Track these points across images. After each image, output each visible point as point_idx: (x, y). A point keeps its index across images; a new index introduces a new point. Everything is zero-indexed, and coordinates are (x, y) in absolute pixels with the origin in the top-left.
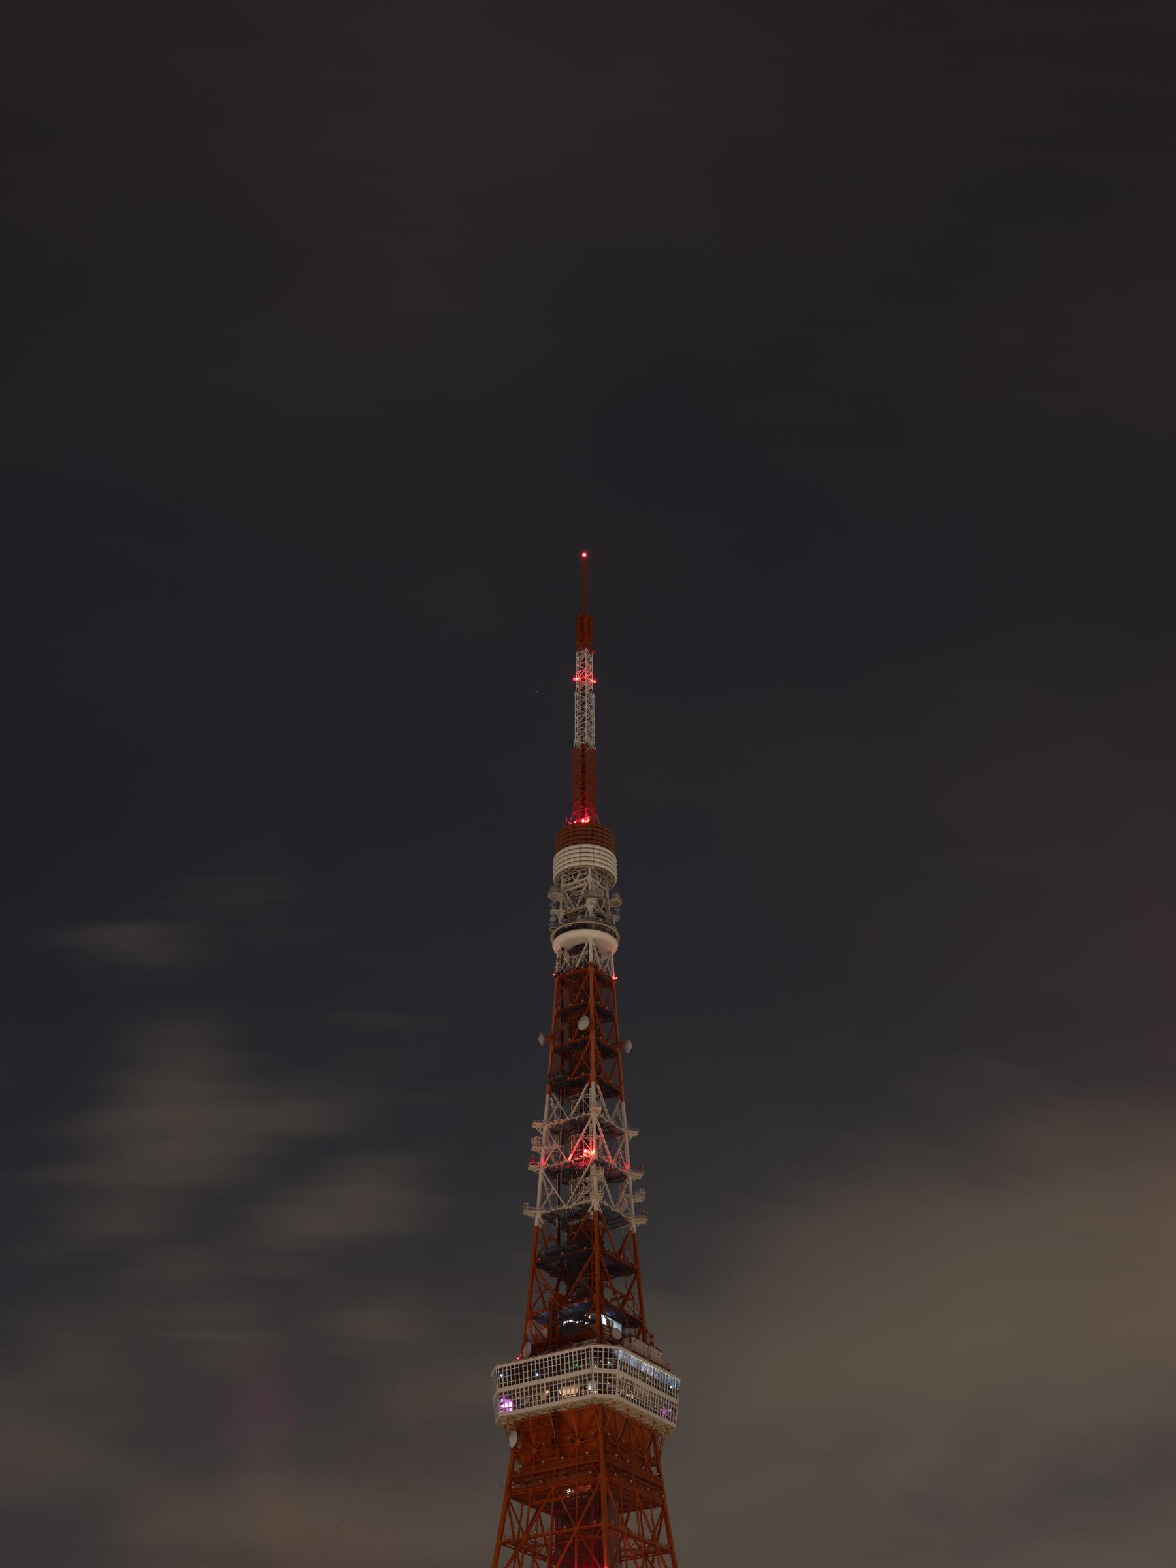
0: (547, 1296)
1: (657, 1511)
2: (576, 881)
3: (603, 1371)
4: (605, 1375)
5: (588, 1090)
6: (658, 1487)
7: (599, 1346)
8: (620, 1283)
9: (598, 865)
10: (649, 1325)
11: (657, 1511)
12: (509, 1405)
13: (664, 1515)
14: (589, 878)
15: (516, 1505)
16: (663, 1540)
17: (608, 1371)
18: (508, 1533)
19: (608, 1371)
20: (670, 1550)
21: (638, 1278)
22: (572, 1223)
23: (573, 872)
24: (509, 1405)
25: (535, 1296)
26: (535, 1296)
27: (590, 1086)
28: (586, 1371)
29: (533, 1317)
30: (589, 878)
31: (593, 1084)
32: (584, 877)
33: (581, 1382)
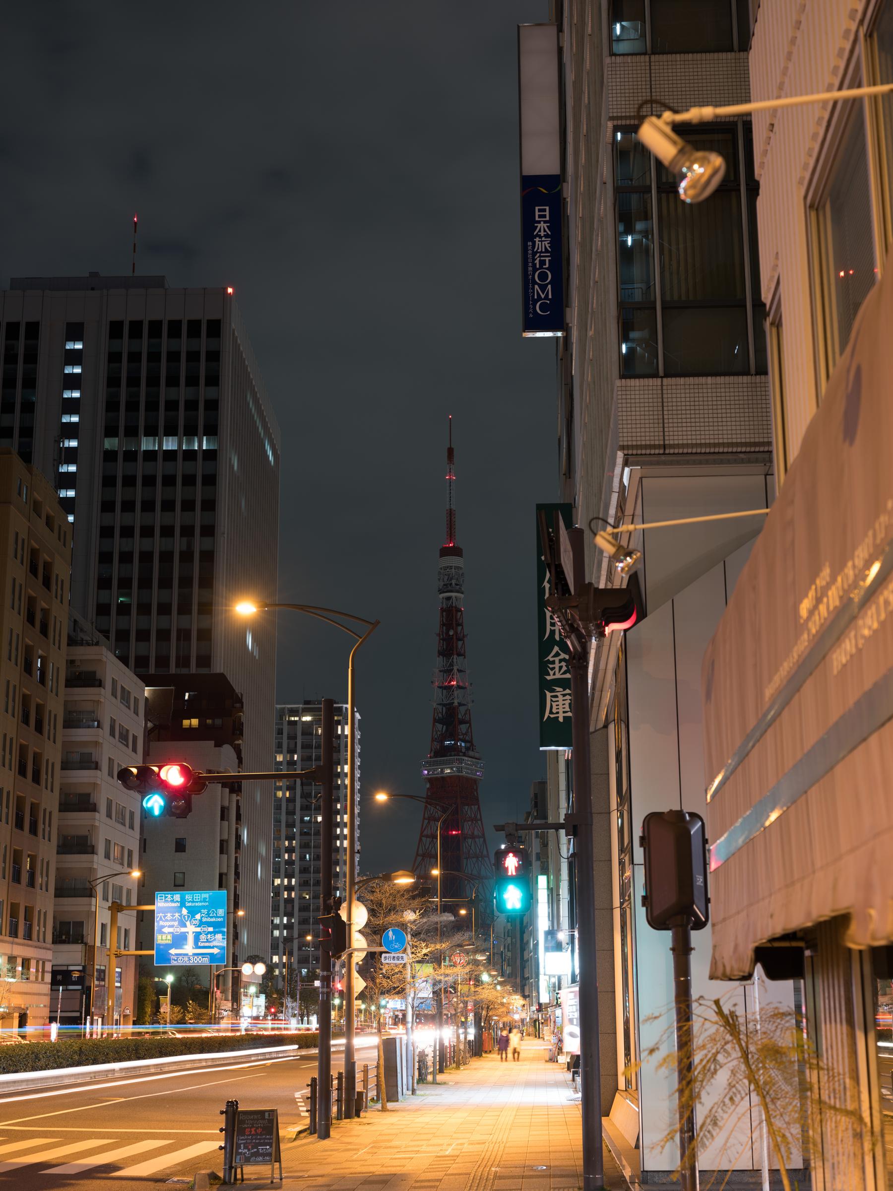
0: (439, 733)
1: (477, 807)
6: (477, 800)
8: (463, 728)
10: (475, 742)
11: (477, 807)
12: (426, 772)
13: (479, 808)
15: (429, 806)
16: (479, 817)
18: (426, 816)
20: (481, 820)
21: (470, 726)
23: (445, 568)
24: (426, 772)
25: (434, 733)
26: (434, 733)
29: (433, 740)
33: (451, 769)
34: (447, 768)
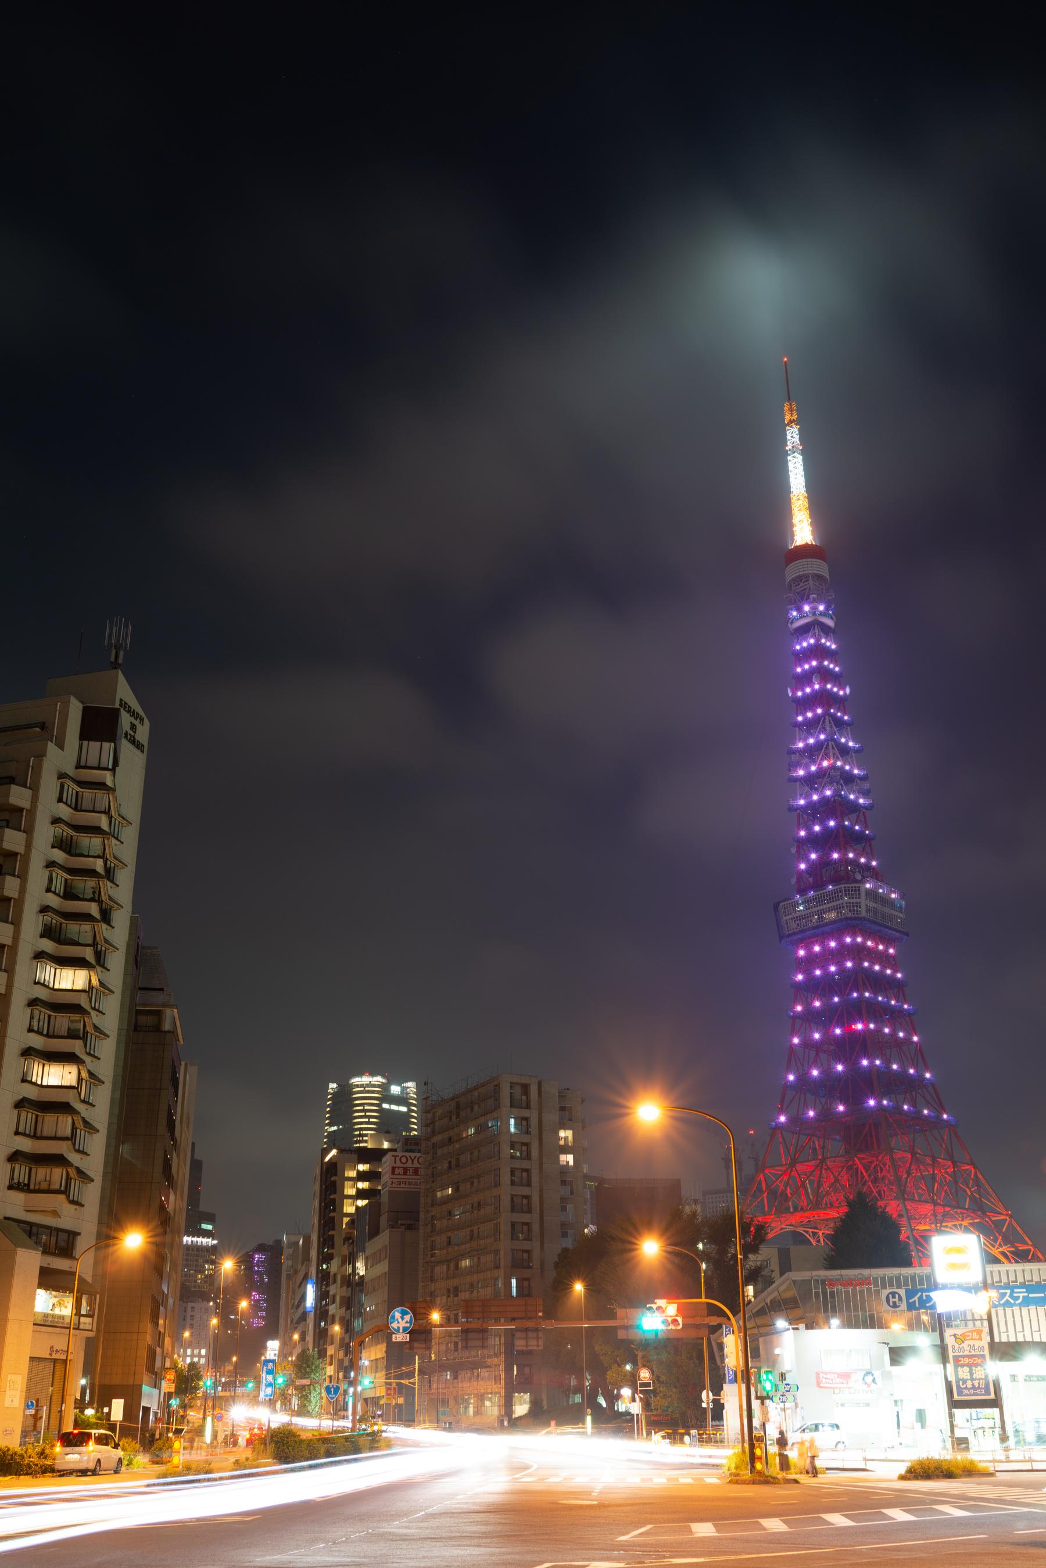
2: (801, 585)
3: (851, 900)
4: (853, 903)
5: (824, 722)
7: (847, 885)
9: (815, 572)
14: (811, 582)
17: (854, 900)
19: (854, 900)
22: (821, 809)
23: (799, 579)
27: (825, 719)
28: (838, 903)
30: (811, 582)
31: (827, 717)
32: (807, 581)
34: (829, 911)
